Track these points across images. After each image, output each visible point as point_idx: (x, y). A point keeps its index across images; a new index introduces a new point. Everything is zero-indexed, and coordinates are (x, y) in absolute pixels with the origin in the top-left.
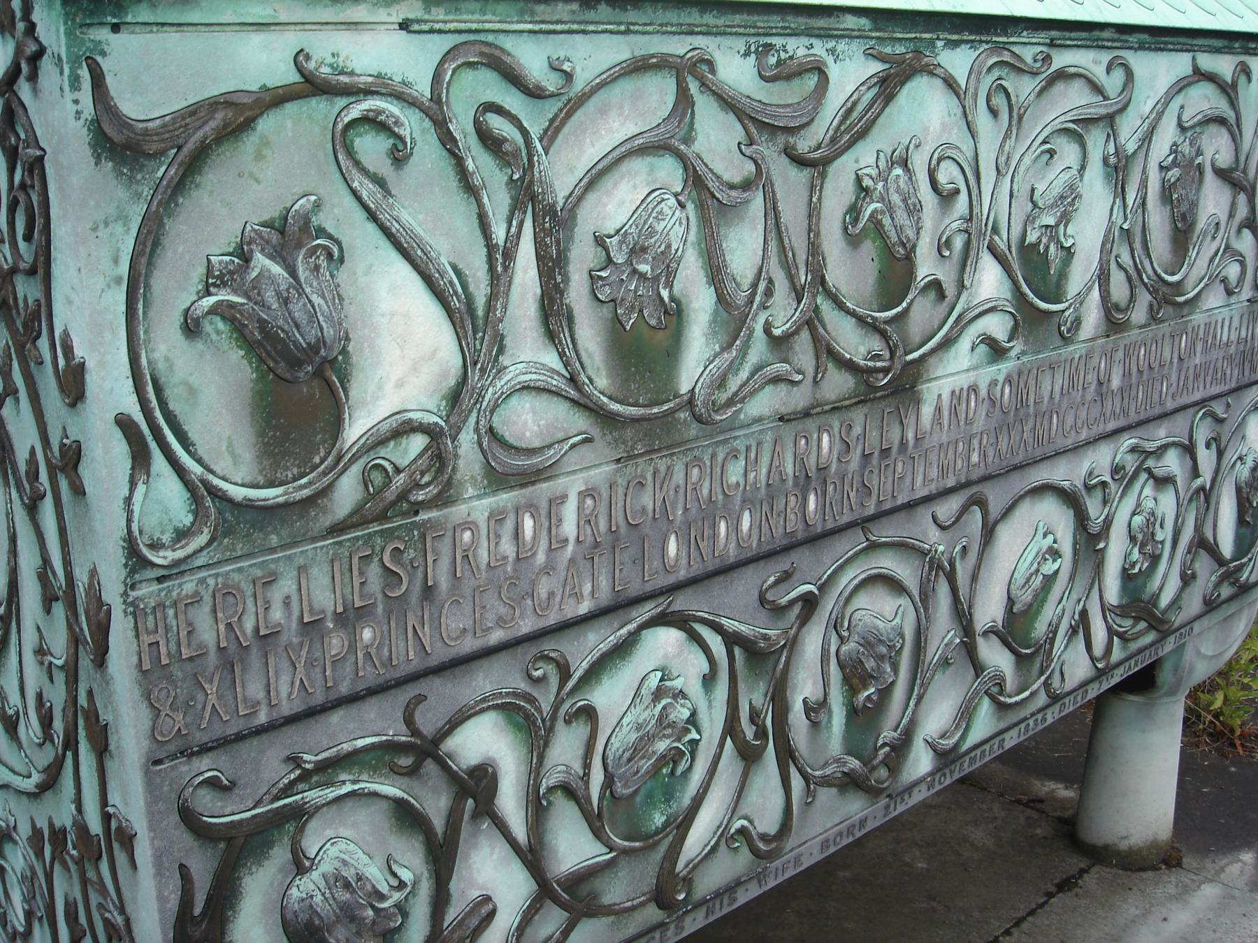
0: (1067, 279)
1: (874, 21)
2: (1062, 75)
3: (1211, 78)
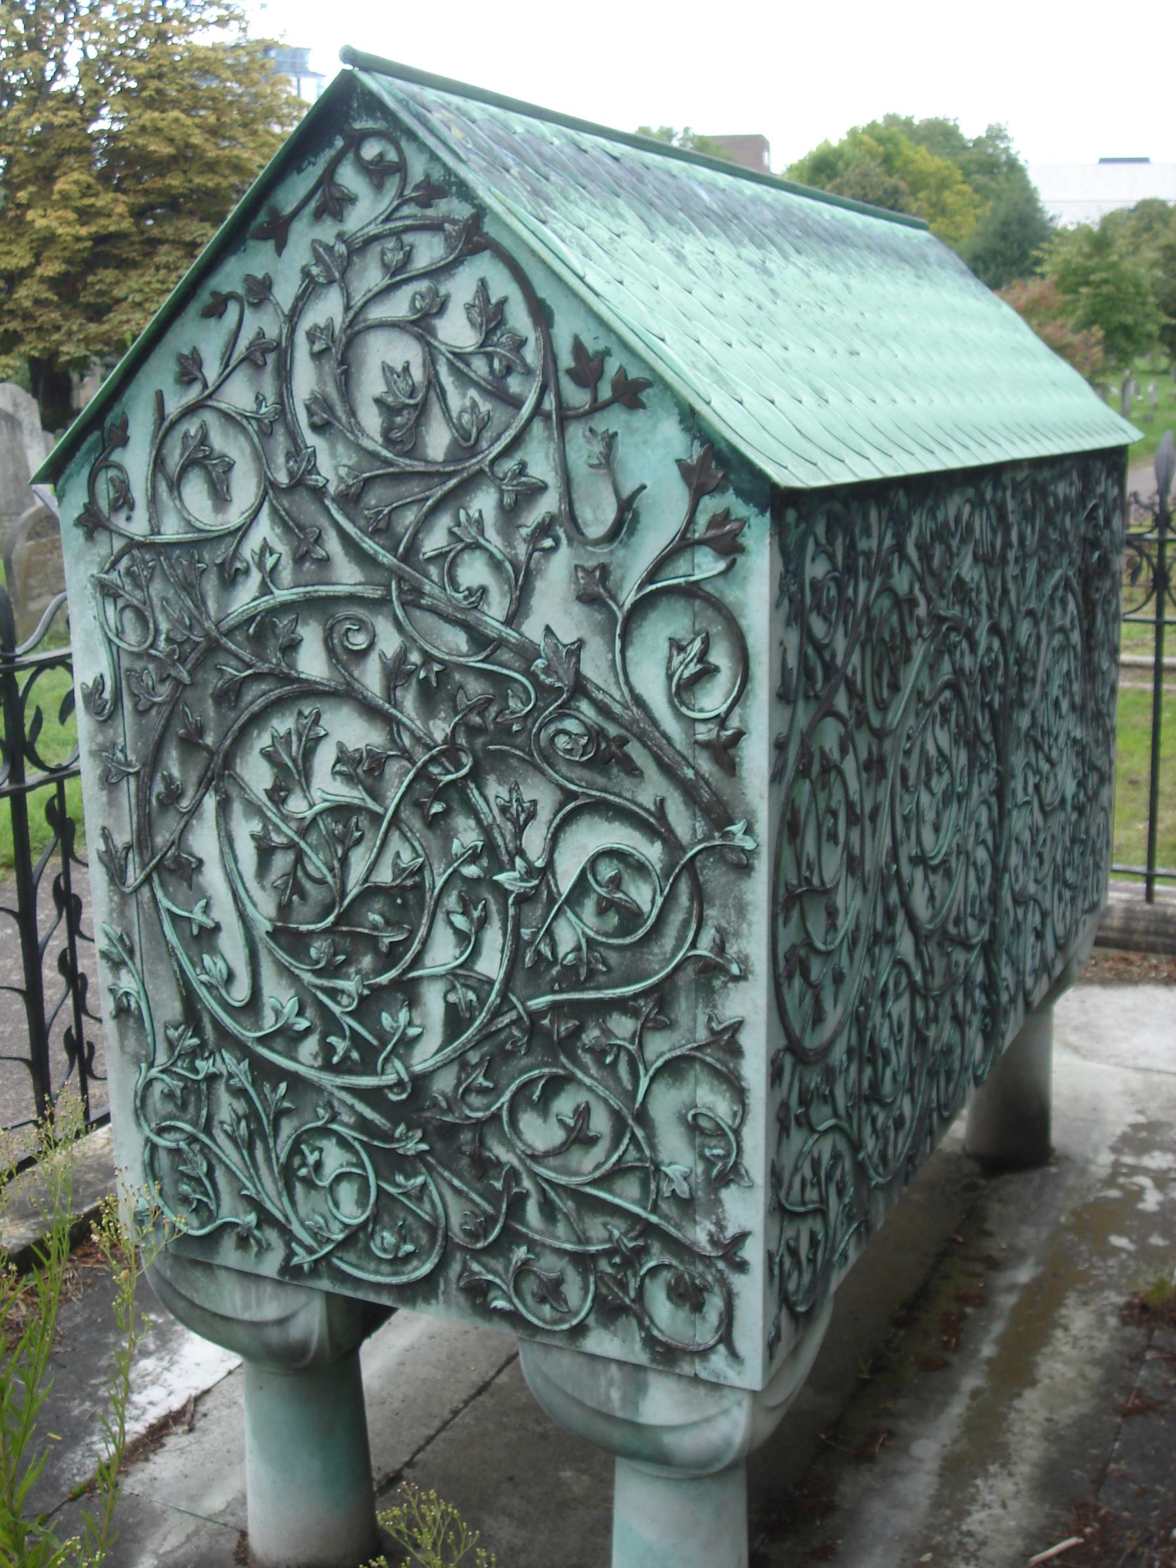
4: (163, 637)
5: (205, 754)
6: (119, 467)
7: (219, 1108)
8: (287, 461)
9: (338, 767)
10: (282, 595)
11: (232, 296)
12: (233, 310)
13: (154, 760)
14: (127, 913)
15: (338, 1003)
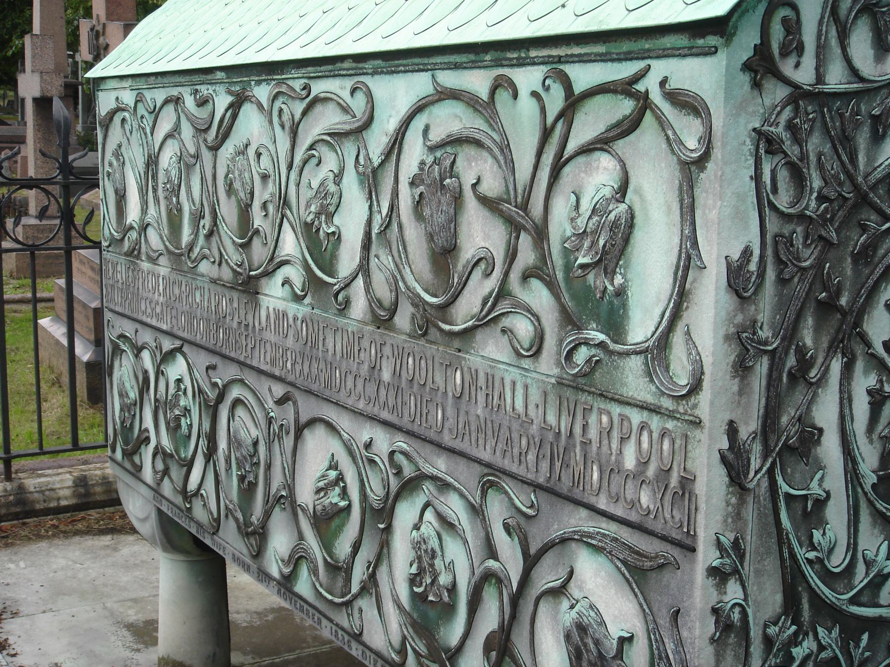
0: (337, 259)
1: (227, 74)
2: (317, 100)
3: (454, 95)
4: (815, 195)
5: (839, 316)
13: (791, 334)
14: (744, 513)
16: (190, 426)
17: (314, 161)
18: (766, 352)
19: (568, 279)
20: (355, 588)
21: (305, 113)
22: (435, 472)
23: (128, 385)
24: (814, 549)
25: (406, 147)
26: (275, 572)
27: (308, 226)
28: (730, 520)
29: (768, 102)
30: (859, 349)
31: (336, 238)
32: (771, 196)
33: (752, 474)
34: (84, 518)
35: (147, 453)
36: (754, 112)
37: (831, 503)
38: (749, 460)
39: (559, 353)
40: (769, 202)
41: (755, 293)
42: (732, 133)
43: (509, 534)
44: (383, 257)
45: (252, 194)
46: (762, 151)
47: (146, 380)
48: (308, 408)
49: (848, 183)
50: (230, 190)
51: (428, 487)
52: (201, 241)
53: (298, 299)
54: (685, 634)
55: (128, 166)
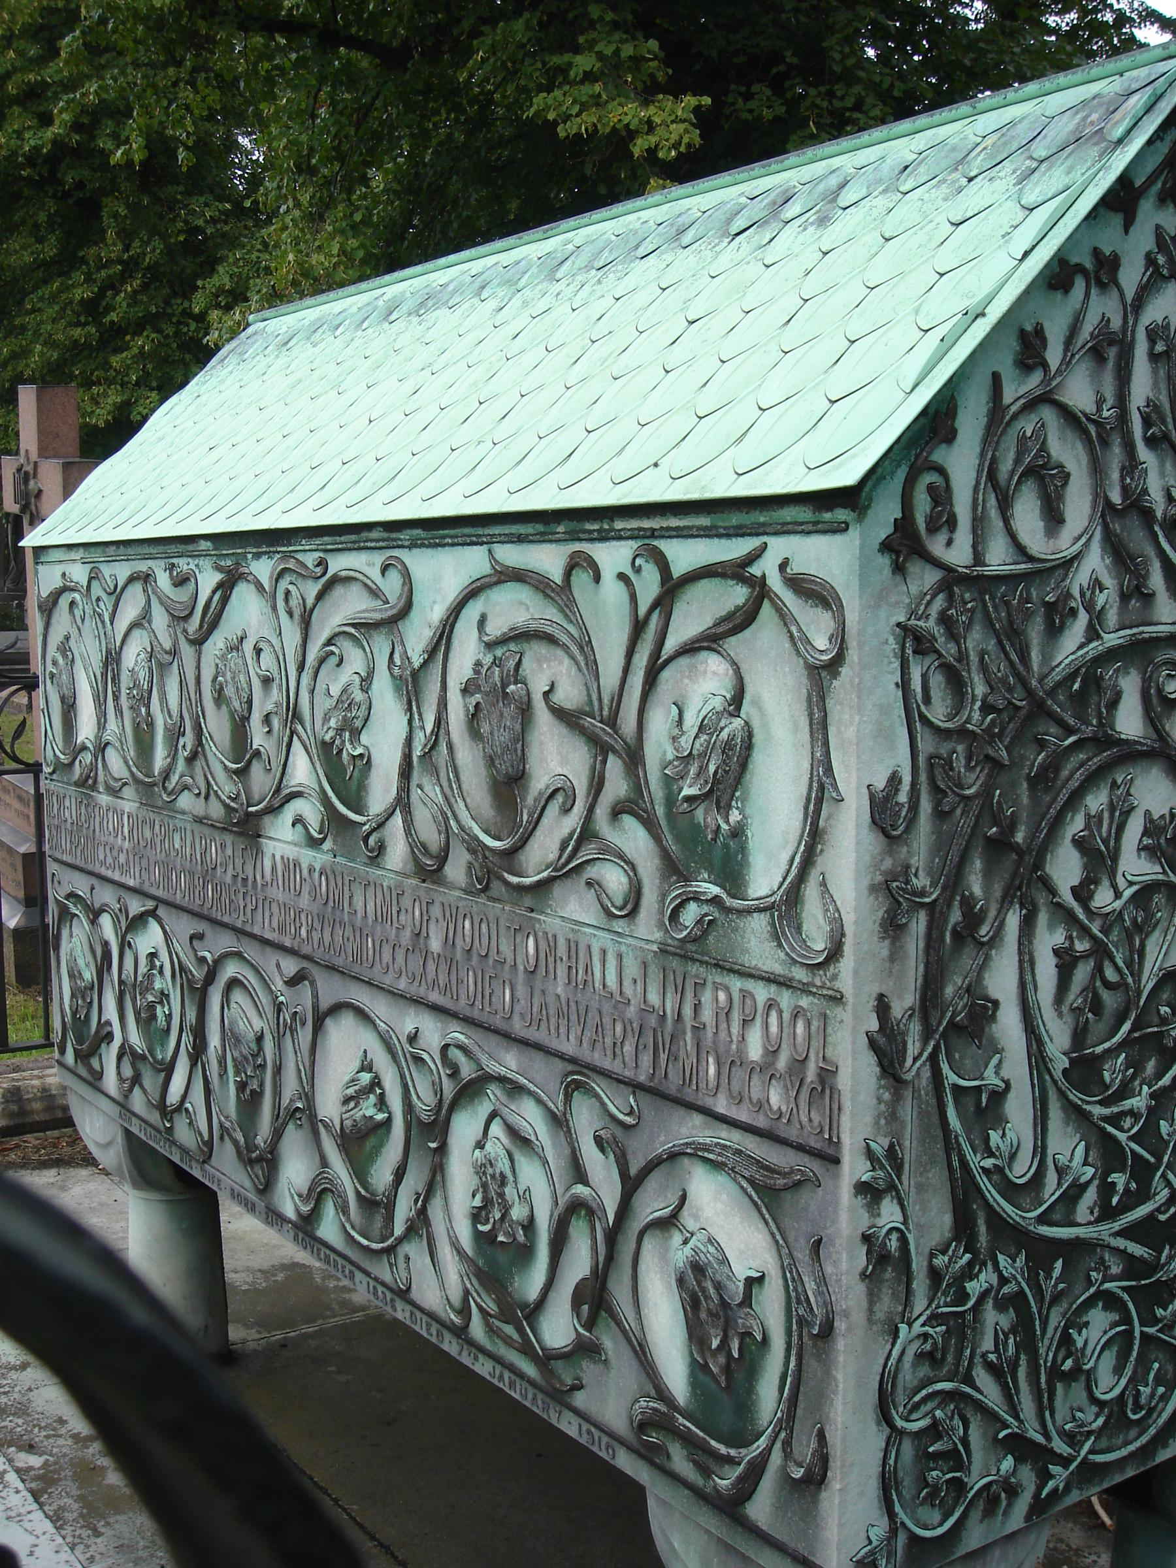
1: (214, 543)
2: (335, 580)
3: (518, 576)
4: (979, 704)
5: (1014, 856)
6: (941, 471)
7: (982, 1333)
8: (1122, 478)
9: (1147, 841)
10: (1111, 639)
11: (1080, 269)
12: (1079, 284)
13: (954, 882)
14: (900, 1112)
15: (1121, 1130)
16: (169, 1017)
17: (333, 660)
18: (923, 905)
19: (670, 816)
20: (399, 1229)
21: (320, 596)
22: (503, 1071)
23: (81, 962)
24: (991, 1154)
25: (455, 642)
26: (289, 1212)
27: (326, 746)
28: (883, 1121)
29: (914, 589)
30: (1042, 898)
31: (365, 762)
32: (923, 708)
33: (909, 1061)
34: (17, 1146)
35: (110, 1054)
36: (898, 603)
37: (1011, 1095)
38: (905, 1043)
39: (662, 912)
40: (921, 715)
41: (907, 830)
42: (870, 630)
43: (602, 1150)
44: (428, 788)
45: (250, 702)
46: (909, 651)
47: (107, 954)
48: (330, 990)
49: (1019, 688)
50: (220, 698)
51: (494, 1091)
52: (181, 765)
53: (314, 843)
54: (829, 1269)
55: (79, 665)
